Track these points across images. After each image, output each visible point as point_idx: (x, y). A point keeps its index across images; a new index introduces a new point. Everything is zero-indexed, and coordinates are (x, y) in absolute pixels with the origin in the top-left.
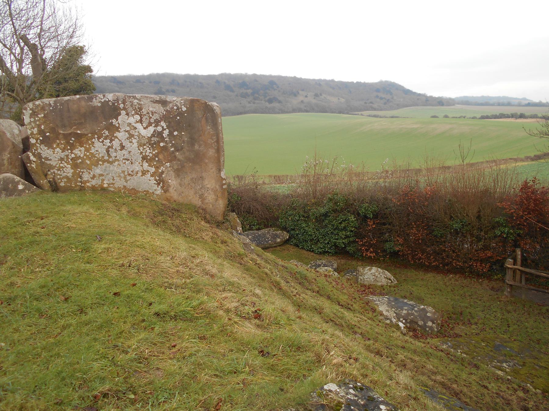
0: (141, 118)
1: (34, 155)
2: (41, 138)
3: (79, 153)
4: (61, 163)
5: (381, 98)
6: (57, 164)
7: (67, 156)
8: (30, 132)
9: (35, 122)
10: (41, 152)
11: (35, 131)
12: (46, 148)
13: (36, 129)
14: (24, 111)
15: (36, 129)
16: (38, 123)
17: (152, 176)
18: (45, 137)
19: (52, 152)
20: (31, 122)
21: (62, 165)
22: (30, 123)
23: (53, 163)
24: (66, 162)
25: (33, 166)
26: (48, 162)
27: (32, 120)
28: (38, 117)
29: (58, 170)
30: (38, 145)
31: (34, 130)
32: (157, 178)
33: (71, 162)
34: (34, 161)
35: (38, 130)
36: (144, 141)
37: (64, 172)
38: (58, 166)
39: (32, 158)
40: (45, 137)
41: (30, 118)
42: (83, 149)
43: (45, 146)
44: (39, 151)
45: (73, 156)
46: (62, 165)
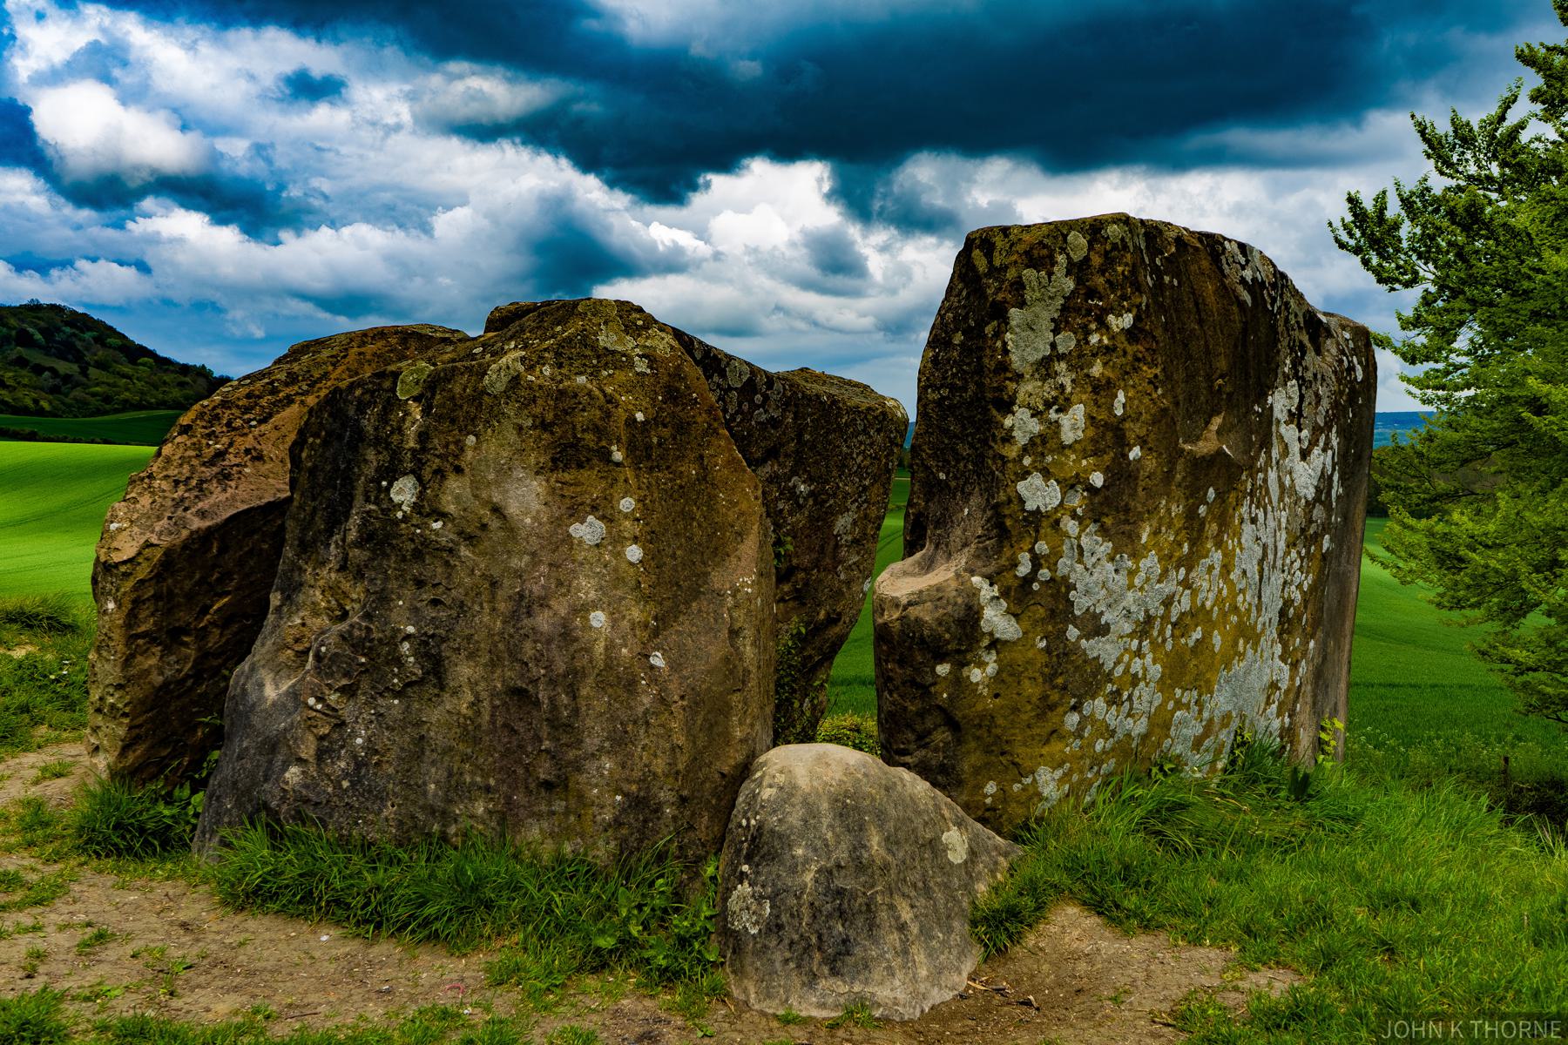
0: (1302, 397)
1: (1018, 596)
2: (1098, 479)
3: (1205, 585)
4: (1139, 653)
5: (38, 370)
6: (1118, 662)
7: (1168, 602)
8: (1035, 426)
9: (1078, 360)
10: (1077, 574)
11: (1073, 423)
12: (1106, 547)
13: (1078, 412)
14: (1029, 274)
15: (1078, 412)
16: (1097, 370)
17: (1279, 714)
18: (1121, 474)
19: (1122, 579)
20: (1055, 356)
21: (1137, 665)
22: (1045, 368)
23: (1104, 650)
24: (1155, 646)
25: (976, 675)
26: (1096, 648)
27: (1067, 342)
28: (1103, 326)
29: (1114, 699)
30: (1071, 526)
31: (1066, 421)
32: (1287, 720)
33: (1169, 646)
34: (995, 644)
35: (1091, 419)
36: (1296, 527)
37: (1129, 715)
38: (1120, 669)
39: (996, 619)
40: (1121, 474)
41: (1056, 332)
42: (1217, 557)
43: (1104, 532)
44: (1064, 565)
45: (1185, 603)
46: (1137, 665)
